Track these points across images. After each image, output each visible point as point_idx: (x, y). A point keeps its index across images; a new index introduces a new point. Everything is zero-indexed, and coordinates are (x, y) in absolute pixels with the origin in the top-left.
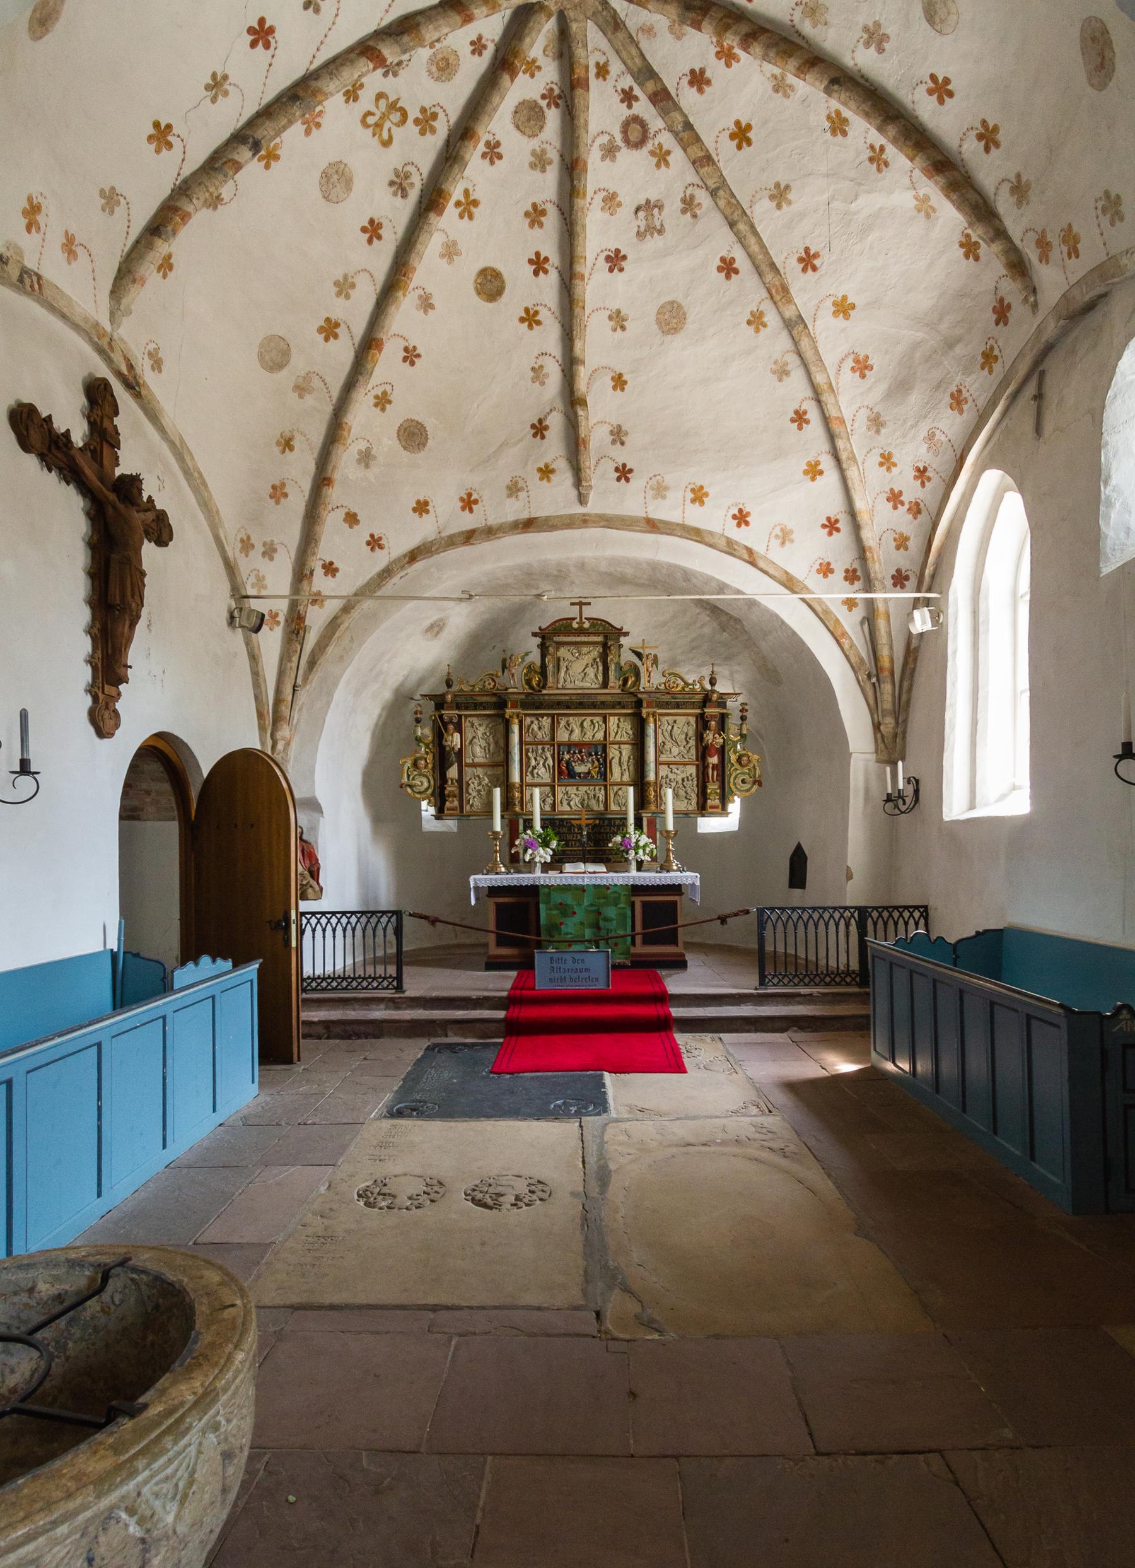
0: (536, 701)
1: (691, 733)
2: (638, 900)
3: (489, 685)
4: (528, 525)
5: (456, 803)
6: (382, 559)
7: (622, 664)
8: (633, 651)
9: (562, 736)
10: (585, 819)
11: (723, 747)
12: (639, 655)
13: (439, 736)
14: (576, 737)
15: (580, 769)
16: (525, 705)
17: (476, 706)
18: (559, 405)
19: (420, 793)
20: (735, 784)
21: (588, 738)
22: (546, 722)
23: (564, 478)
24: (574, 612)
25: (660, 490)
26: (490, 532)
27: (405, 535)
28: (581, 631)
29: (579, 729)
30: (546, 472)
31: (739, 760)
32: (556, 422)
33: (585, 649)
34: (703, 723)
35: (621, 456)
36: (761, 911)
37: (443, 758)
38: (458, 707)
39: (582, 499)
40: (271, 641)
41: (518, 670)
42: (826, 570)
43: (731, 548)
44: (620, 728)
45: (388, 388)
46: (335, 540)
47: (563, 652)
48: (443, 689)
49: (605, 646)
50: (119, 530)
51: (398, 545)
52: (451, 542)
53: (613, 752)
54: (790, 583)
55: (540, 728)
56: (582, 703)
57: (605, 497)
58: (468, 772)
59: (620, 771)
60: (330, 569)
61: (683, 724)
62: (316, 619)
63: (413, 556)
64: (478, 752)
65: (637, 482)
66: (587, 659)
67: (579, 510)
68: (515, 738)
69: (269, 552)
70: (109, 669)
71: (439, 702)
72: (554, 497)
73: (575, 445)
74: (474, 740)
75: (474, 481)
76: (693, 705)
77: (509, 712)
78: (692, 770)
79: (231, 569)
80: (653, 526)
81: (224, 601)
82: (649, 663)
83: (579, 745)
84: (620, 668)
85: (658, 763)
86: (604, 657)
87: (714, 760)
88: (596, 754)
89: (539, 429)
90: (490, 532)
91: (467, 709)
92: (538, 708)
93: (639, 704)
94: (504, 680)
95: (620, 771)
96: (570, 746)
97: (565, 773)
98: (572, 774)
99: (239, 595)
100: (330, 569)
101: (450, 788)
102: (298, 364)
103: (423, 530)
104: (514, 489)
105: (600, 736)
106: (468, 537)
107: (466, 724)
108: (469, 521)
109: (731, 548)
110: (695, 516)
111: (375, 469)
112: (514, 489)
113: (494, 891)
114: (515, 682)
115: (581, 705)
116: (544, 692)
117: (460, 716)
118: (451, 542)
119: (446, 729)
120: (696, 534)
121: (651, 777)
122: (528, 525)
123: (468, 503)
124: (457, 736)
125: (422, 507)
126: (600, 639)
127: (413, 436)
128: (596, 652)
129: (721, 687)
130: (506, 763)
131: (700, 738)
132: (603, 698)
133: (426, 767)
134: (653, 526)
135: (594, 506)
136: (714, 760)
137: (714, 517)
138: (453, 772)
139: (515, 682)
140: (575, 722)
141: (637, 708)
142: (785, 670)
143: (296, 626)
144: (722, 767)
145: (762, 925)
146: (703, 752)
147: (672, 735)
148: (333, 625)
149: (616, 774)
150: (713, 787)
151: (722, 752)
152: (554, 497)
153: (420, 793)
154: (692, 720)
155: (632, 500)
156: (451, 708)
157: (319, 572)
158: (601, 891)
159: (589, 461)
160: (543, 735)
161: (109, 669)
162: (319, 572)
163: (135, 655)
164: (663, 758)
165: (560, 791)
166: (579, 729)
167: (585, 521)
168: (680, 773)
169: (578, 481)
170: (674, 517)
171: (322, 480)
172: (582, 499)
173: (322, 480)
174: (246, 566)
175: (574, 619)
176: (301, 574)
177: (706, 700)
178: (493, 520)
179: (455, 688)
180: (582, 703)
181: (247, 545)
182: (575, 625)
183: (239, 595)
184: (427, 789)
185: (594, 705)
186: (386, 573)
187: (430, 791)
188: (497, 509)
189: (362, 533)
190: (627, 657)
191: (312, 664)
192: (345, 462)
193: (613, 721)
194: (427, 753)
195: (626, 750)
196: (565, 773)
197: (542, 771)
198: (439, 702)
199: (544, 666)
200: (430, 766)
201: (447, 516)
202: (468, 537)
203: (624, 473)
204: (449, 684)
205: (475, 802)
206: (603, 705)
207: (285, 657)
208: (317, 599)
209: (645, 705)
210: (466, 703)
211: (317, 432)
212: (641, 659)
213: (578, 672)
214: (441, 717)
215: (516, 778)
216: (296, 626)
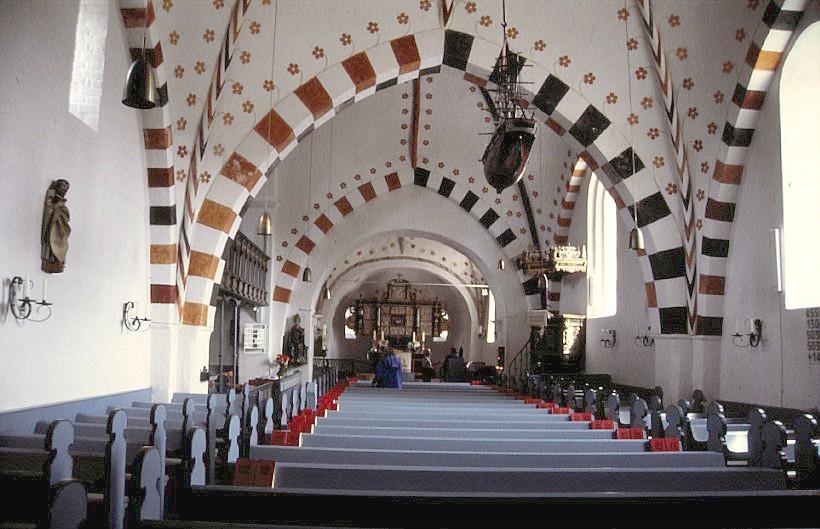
0: (386, 302)
4: (388, 258)
6: (348, 266)
9: (392, 312)
10: (398, 337)
25: (423, 251)
26: (377, 260)
29: (396, 310)
30: (392, 245)
34: (434, 309)
41: (381, 294)
42: (466, 274)
43: (441, 266)
44: (409, 310)
47: (394, 288)
48: (358, 297)
52: (367, 262)
53: (407, 318)
54: (456, 276)
59: (409, 323)
61: (428, 310)
63: (356, 265)
64: (368, 316)
72: (395, 252)
77: (378, 305)
78: (431, 324)
80: (420, 260)
86: (406, 290)
90: (377, 260)
93: (415, 304)
94: (376, 296)
95: (409, 323)
96: (395, 315)
97: (393, 323)
103: (359, 259)
104: (384, 249)
108: (372, 257)
109: (441, 266)
110: (431, 258)
118: (367, 262)
122: (388, 258)
123: (371, 252)
134: (420, 260)
135: (405, 255)
136: (437, 321)
137: (436, 258)
138: (361, 322)
141: (414, 304)
142: (454, 295)
146: (434, 318)
147: (424, 314)
150: (436, 329)
151: (439, 319)
152: (395, 252)
155: (415, 253)
166: (396, 310)
168: (427, 324)
169: (401, 248)
170: (426, 258)
178: (378, 257)
180: (399, 303)
190: (413, 292)
196: (393, 323)
198: (358, 302)
199: (388, 293)
201: (366, 256)
202: (372, 261)
203: (413, 246)
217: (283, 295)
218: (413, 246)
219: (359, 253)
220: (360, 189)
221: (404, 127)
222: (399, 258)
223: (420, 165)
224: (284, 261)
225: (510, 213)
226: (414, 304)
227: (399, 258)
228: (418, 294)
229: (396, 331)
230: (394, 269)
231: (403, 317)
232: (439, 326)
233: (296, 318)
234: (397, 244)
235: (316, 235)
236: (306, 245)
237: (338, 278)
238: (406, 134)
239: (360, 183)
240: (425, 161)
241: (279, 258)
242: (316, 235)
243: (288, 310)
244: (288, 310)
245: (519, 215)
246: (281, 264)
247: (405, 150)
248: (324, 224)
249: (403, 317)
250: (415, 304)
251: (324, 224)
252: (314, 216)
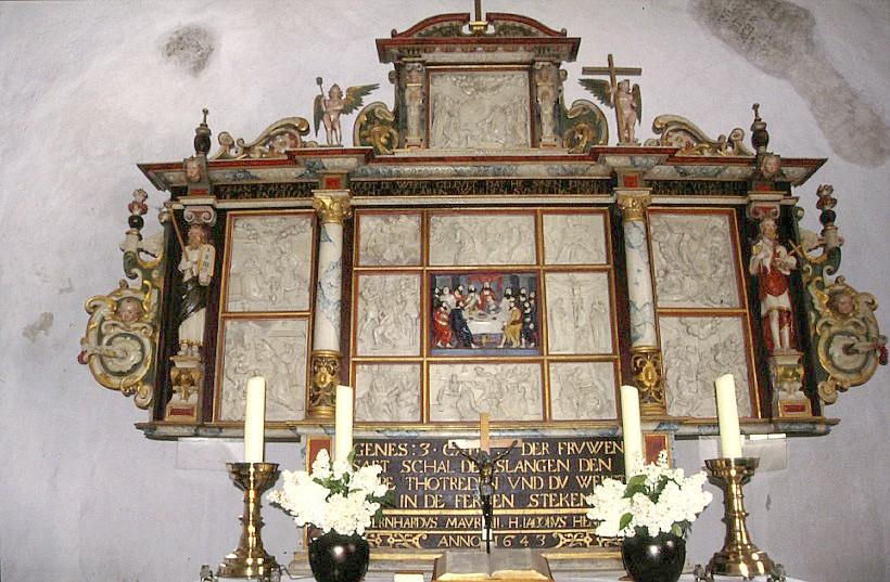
5: (194, 399)
7: (568, 106)
8: (588, 84)
11: (797, 273)
12: (597, 88)
13: (173, 253)
19: (121, 374)
20: (829, 357)
28: (480, 39)
31: (832, 304)
33: (489, 79)
38: (219, 191)
47: (443, 86)
53: (556, 289)
78: (733, 329)
82: (625, 100)
85: (659, 314)
88: (516, 293)
91: (235, 196)
92: (387, 193)
97: (446, 332)
101: (186, 363)
115: (481, 187)
116: (401, 153)
117: (221, 213)
119: (185, 237)
124: (209, 251)
126: (521, 55)
132: (526, 171)
133: (139, 315)
138: (193, 329)
144: (799, 315)
146: (754, 288)
149: (560, 336)
151: (795, 284)
153: (121, 374)
156: (202, 193)
164: (665, 302)
175: (465, 18)
179: (215, 150)
182: (465, 30)
184: (136, 367)
187: (142, 372)
194: (145, 289)
196: (446, 332)
200: (149, 317)
204: (203, 142)
209: (620, 181)
212: (605, 98)
214: (179, 214)
231: (523, 288)
249: (523, 288)
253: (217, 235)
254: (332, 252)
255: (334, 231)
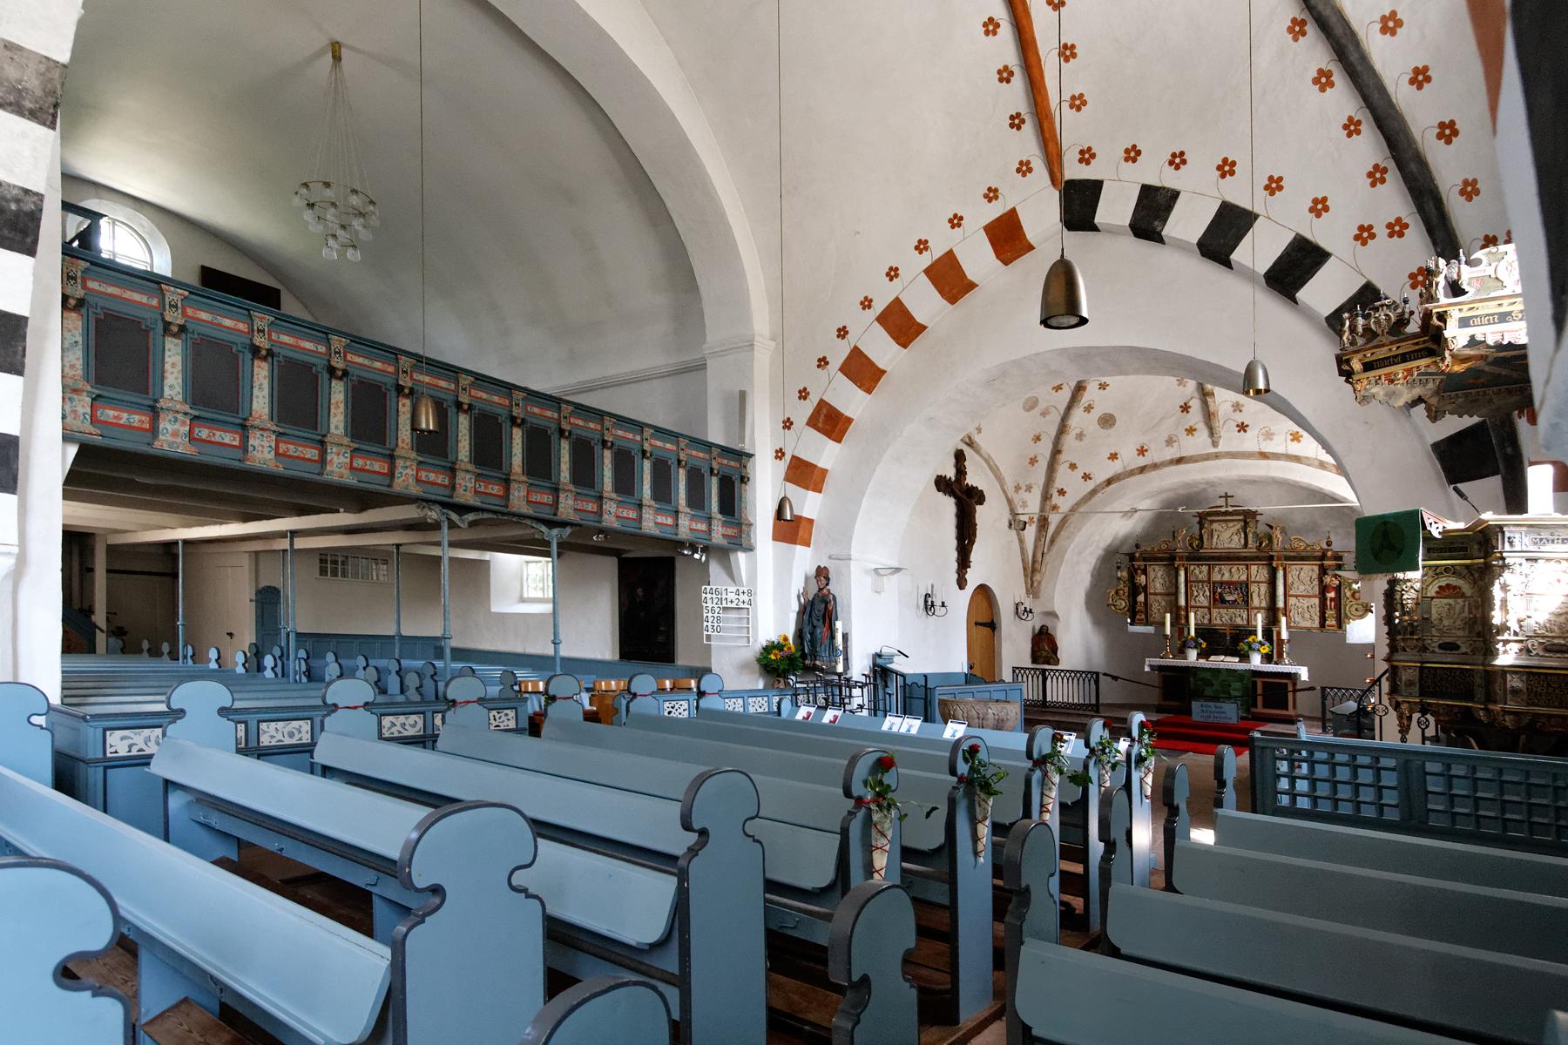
0: (1196, 557)
1: (1315, 576)
2: (1259, 681)
3: (1164, 547)
4: (1180, 461)
6: (1090, 485)
9: (1216, 577)
11: (1339, 586)
13: (1132, 577)
14: (1226, 577)
15: (1228, 598)
16: (1188, 559)
17: (1156, 559)
18: (1196, 395)
21: (1235, 578)
22: (1205, 569)
23: (1202, 434)
24: (1222, 502)
25: (1269, 436)
26: (1155, 466)
27: (1102, 473)
29: (1224, 573)
30: (1191, 431)
32: (1195, 404)
34: (1323, 571)
35: (1240, 418)
36: (1323, 689)
37: (1135, 590)
39: (1215, 444)
40: (1030, 533)
45: (1048, 622)
46: (1063, 477)
47: (1215, 526)
49: (1246, 523)
50: (966, 499)
51: (1100, 477)
52: (1131, 473)
53: (1253, 588)
55: (1200, 572)
56: (1230, 558)
57: (1230, 440)
58: (1151, 598)
60: (1062, 492)
62: (1054, 520)
63: (1109, 482)
65: (1251, 433)
66: (1234, 530)
67: (1214, 450)
68: (1182, 578)
69: (1029, 489)
70: (964, 562)
71: (1132, 557)
73: (1209, 417)
74: (1156, 578)
75: (1143, 440)
76: (1315, 558)
78: (1316, 601)
79: (1010, 502)
80: (1264, 456)
81: (1007, 516)
83: (1229, 583)
84: (1256, 535)
86: (1244, 529)
87: (1332, 595)
89: (1185, 408)
90: (1155, 466)
93: (1271, 558)
94: (1172, 545)
96: (1222, 583)
97: (1218, 601)
98: (1223, 601)
99: (1014, 513)
100: (1062, 492)
102: (1042, 406)
103: (1116, 467)
104: (1170, 442)
105: (1244, 578)
106: (1142, 470)
107: (1150, 570)
108: (1142, 461)
111: (1086, 440)
112: (1170, 442)
113: (1161, 668)
114: (1181, 547)
118: (1131, 473)
120: (1297, 459)
121: (1281, 604)
122: (1180, 461)
123: (1142, 451)
125: (1113, 457)
127: (1107, 421)
128: (1239, 525)
129: (1336, 547)
130: (1176, 594)
131: (1321, 581)
134: (1264, 456)
135: (1222, 448)
138: (1141, 598)
139: (1181, 547)
140: (1225, 569)
143: (1043, 523)
145: (1324, 697)
146: (1324, 589)
148: (1064, 521)
149: (1256, 602)
151: (1338, 589)
152: (1199, 443)
154: (1316, 568)
155: (1250, 442)
157: (1055, 494)
158: (1231, 672)
159: (1218, 424)
160: (1203, 576)
161: (964, 562)
162: (1055, 494)
163: (973, 557)
165: (1215, 612)
166: (1224, 573)
167: (1217, 456)
168: (1306, 602)
169: (1212, 434)
170: (1280, 450)
171: (1056, 452)
172: (1215, 444)
173: (1056, 452)
174: (1016, 499)
176: (1046, 497)
177: (1323, 557)
178: (1157, 460)
180: (1230, 558)
181: (1017, 488)
183: (1014, 513)
185: (1238, 559)
186: (1094, 492)
188: (1158, 453)
189: (1079, 473)
190: (1262, 529)
191: (1052, 541)
192: (1069, 441)
193: (1254, 568)
195: (1264, 587)
196: (1218, 601)
197: (1202, 598)
198: (1132, 557)
199: (1201, 536)
201: (1129, 459)
202: (1142, 470)
203: (1242, 427)
205: (1156, 616)
206: (1245, 559)
207: (1037, 539)
208: (1055, 508)
210: (1151, 558)
211: (1053, 431)
213: (1226, 537)
215: (1182, 602)
216: (1043, 523)
217: (791, 529)
218: (1242, 427)
219: (1113, 457)
220: (927, 272)
221: (1005, 76)
222: (1207, 457)
223: (1074, 170)
224: (788, 457)
225: (1364, 234)
226: (1268, 557)
227: (1207, 457)
228: (1278, 535)
229: (1222, 618)
230: (1211, 484)
232: (1338, 608)
233: (822, 573)
234: (1201, 426)
235: (849, 399)
236: (830, 422)
237: (1073, 510)
238: (1015, 96)
239: (926, 260)
240: (1087, 156)
241: (780, 454)
242: (849, 399)
243: (804, 560)
244: (804, 560)
245: (1397, 229)
246: (783, 466)
247: (1026, 143)
248: (862, 371)
249: (1244, 588)
250: (1271, 558)
251: (862, 371)
252: (839, 353)
253: (1145, 572)
254: (1182, 578)
255: (1182, 573)
